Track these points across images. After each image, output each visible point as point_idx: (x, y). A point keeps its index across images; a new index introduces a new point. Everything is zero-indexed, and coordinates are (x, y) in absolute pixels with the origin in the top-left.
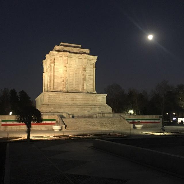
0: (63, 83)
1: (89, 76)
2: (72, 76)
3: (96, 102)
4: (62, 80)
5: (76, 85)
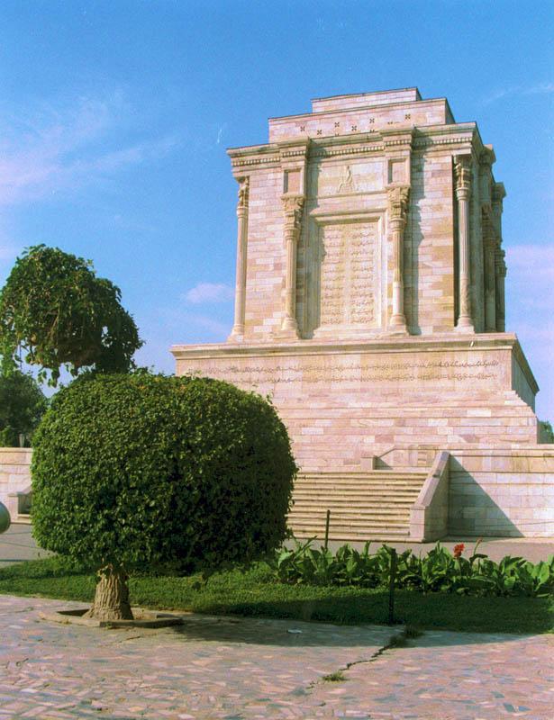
2: (338, 250)
3: (444, 383)
4: (279, 280)
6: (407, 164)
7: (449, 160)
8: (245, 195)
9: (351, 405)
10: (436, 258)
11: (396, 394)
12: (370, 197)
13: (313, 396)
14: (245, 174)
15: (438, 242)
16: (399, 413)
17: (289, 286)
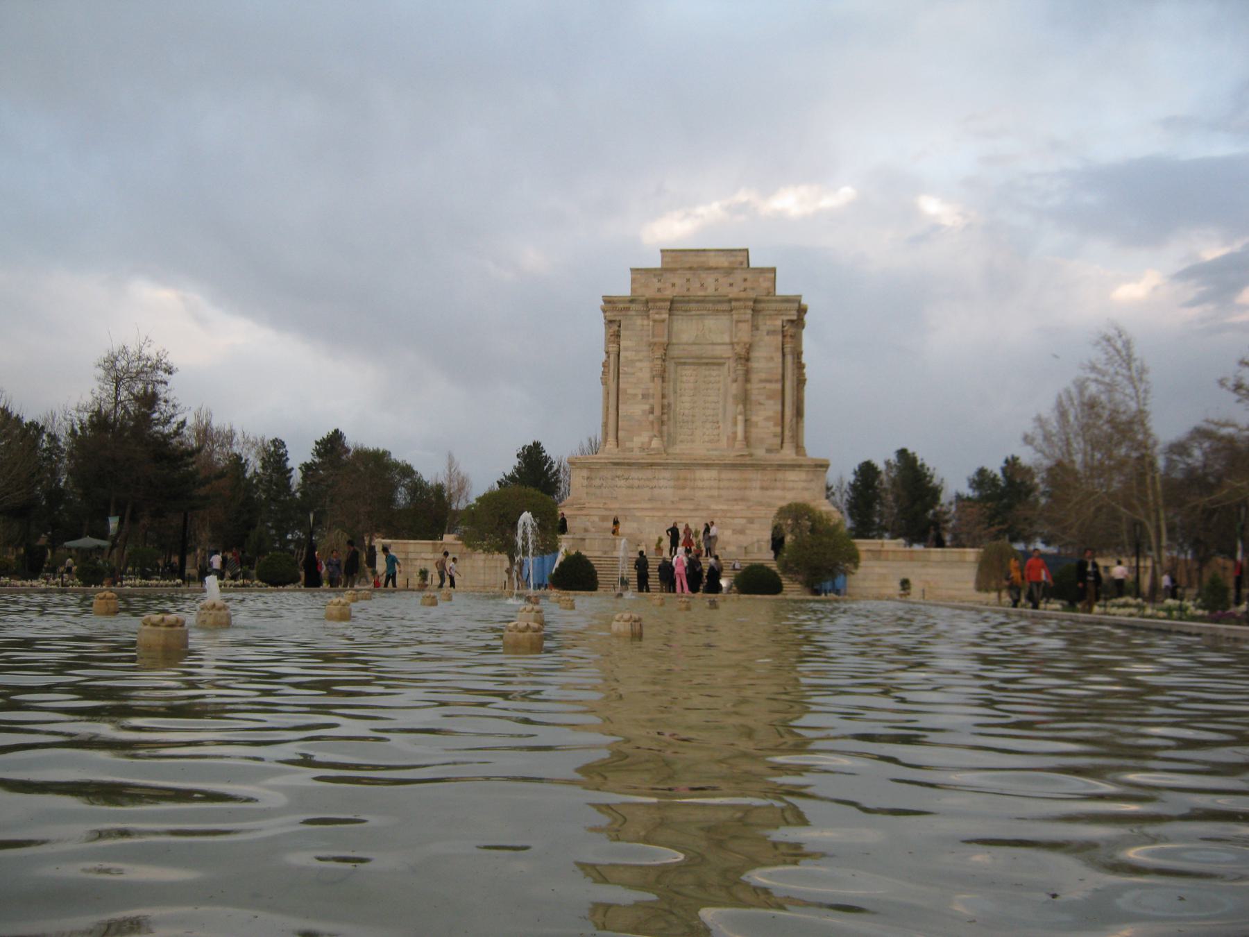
0: (651, 417)
1: (762, 385)
3: (778, 493)
4: (647, 407)
5: (708, 425)
6: (745, 327)
7: (779, 323)
8: (617, 335)
9: (714, 507)
10: (769, 397)
11: (743, 499)
12: (718, 347)
13: (683, 499)
14: (618, 318)
15: (768, 386)
16: (749, 514)
17: (657, 412)
